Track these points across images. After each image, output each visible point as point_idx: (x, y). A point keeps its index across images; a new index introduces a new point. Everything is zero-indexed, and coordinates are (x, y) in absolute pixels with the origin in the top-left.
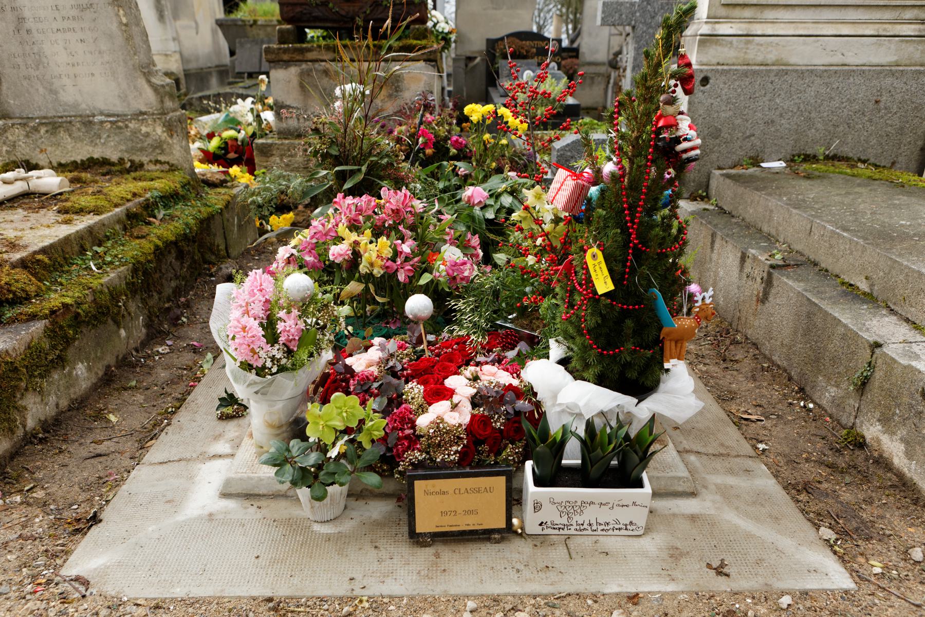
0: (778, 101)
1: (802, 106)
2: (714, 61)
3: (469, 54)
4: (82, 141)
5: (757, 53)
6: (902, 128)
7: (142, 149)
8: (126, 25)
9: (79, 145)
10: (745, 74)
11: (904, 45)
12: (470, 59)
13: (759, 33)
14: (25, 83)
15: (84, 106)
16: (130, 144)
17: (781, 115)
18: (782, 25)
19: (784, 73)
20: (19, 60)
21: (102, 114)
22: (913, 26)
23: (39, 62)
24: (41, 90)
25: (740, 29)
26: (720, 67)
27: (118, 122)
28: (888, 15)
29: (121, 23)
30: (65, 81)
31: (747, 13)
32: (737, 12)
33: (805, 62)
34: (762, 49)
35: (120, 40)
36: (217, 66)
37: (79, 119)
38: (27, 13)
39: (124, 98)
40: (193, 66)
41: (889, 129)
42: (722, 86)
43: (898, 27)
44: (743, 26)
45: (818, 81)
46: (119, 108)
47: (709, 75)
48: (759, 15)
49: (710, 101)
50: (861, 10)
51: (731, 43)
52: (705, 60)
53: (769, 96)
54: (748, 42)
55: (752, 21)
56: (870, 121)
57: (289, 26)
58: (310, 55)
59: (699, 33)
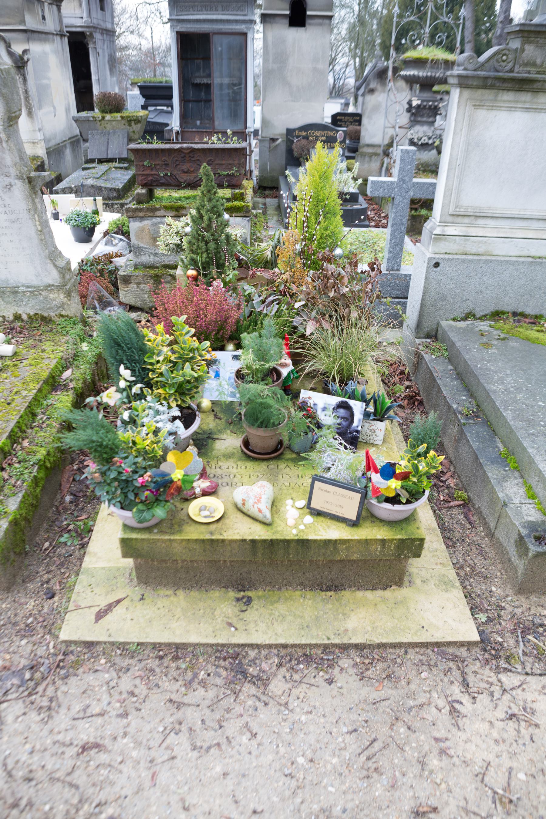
0: (485, 279)
2: (444, 251)
3: (272, 137)
4: (10, 303)
5: (472, 247)
7: (50, 308)
10: (464, 261)
12: (273, 140)
15: (12, 281)
16: (42, 305)
17: (487, 288)
21: (23, 286)
26: (447, 256)
27: (35, 291)
31: (466, 220)
32: (459, 219)
33: (504, 254)
35: (36, 241)
36: (70, 139)
37: (8, 289)
39: (37, 275)
40: (52, 143)
44: (464, 229)
45: (511, 267)
46: (35, 282)
48: (474, 222)
49: (440, 277)
50: (541, 222)
52: (437, 251)
54: (465, 240)
55: (470, 225)
57: (144, 191)
58: (158, 213)
59: (435, 232)
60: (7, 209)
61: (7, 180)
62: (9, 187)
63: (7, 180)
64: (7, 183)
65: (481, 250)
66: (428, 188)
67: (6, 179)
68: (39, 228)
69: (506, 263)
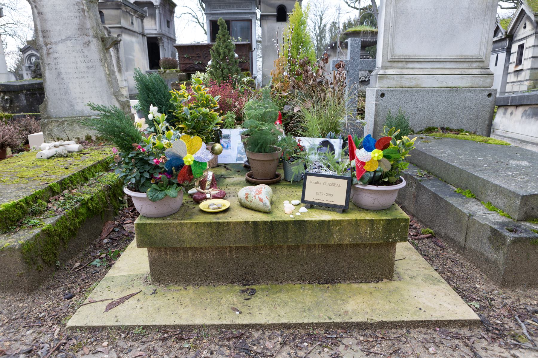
1: (429, 106)
2: (387, 86)
5: (406, 82)
6: (477, 116)
8: (108, 75)
9: (82, 130)
10: (401, 92)
11: (474, 79)
13: (406, 73)
14: (59, 102)
15: (86, 112)
18: (417, 70)
19: (418, 90)
20: (57, 92)
22: (478, 70)
23: (67, 92)
24: (66, 105)
25: (397, 72)
26: (389, 89)
28: (465, 65)
29: (106, 74)
30: (78, 100)
31: (400, 65)
32: (395, 64)
33: (429, 86)
34: (408, 80)
35: (105, 82)
38: (62, 70)
41: (471, 116)
42: (390, 97)
43: (471, 70)
45: (436, 95)
47: (384, 92)
48: (405, 66)
50: (452, 63)
51: (394, 78)
52: (382, 86)
53: (413, 102)
54: (401, 78)
55: (403, 68)
56: (462, 112)
60: (86, 59)
61: (87, 39)
62: (88, 43)
63: (87, 39)
64: (86, 40)
65: (413, 84)
66: (370, 63)
67: (86, 37)
68: (108, 73)
69: (432, 91)
